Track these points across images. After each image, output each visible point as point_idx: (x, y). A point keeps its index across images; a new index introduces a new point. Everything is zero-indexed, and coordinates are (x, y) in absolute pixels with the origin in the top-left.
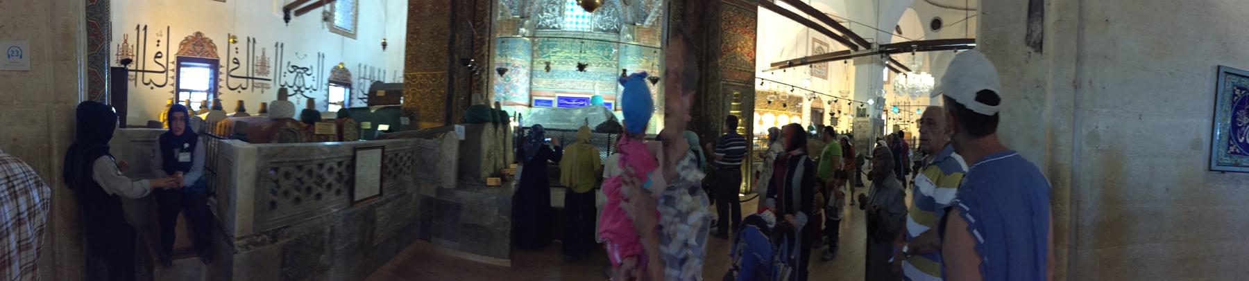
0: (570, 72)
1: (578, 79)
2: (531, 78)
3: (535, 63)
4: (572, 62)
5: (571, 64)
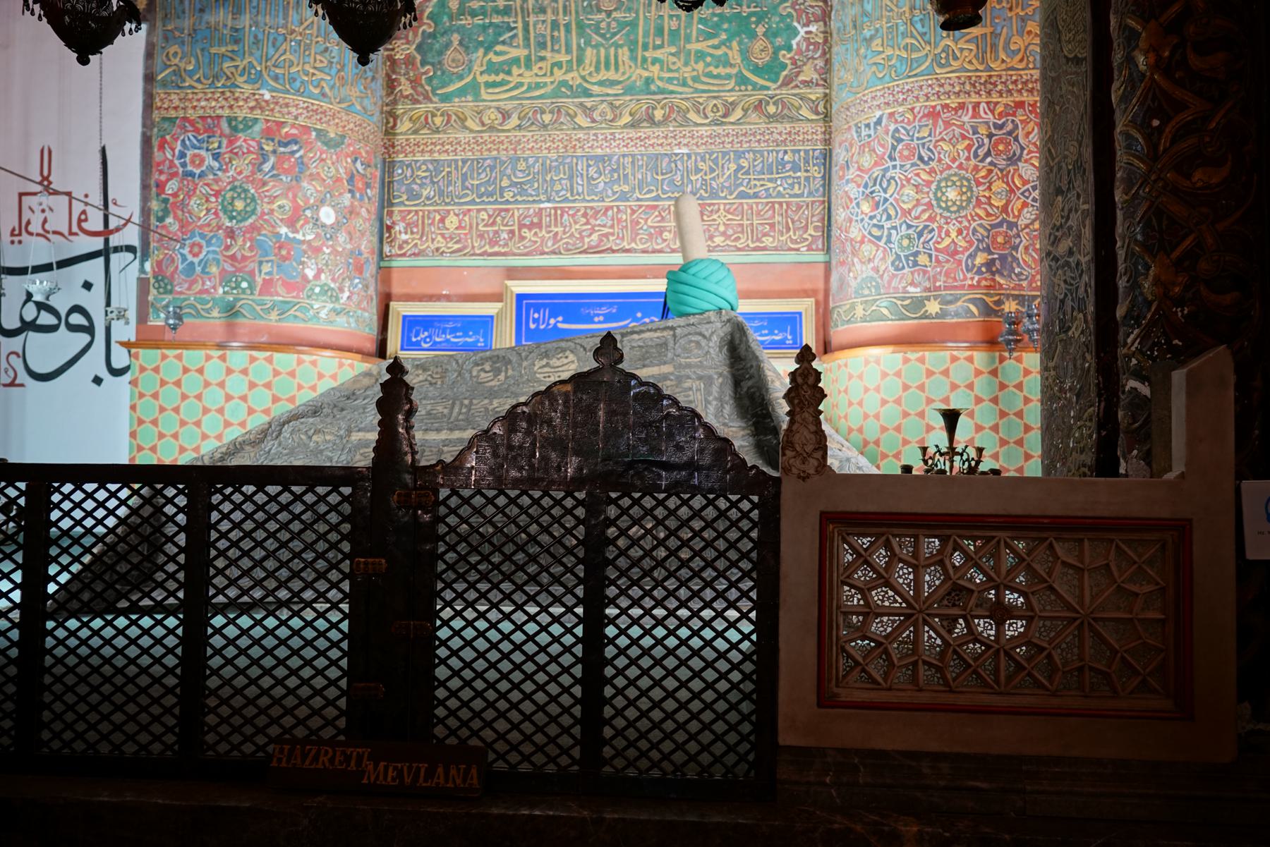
1: (624, 197)
2: (386, 202)
3: (404, 126)
4: (588, 111)
5: (582, 120)
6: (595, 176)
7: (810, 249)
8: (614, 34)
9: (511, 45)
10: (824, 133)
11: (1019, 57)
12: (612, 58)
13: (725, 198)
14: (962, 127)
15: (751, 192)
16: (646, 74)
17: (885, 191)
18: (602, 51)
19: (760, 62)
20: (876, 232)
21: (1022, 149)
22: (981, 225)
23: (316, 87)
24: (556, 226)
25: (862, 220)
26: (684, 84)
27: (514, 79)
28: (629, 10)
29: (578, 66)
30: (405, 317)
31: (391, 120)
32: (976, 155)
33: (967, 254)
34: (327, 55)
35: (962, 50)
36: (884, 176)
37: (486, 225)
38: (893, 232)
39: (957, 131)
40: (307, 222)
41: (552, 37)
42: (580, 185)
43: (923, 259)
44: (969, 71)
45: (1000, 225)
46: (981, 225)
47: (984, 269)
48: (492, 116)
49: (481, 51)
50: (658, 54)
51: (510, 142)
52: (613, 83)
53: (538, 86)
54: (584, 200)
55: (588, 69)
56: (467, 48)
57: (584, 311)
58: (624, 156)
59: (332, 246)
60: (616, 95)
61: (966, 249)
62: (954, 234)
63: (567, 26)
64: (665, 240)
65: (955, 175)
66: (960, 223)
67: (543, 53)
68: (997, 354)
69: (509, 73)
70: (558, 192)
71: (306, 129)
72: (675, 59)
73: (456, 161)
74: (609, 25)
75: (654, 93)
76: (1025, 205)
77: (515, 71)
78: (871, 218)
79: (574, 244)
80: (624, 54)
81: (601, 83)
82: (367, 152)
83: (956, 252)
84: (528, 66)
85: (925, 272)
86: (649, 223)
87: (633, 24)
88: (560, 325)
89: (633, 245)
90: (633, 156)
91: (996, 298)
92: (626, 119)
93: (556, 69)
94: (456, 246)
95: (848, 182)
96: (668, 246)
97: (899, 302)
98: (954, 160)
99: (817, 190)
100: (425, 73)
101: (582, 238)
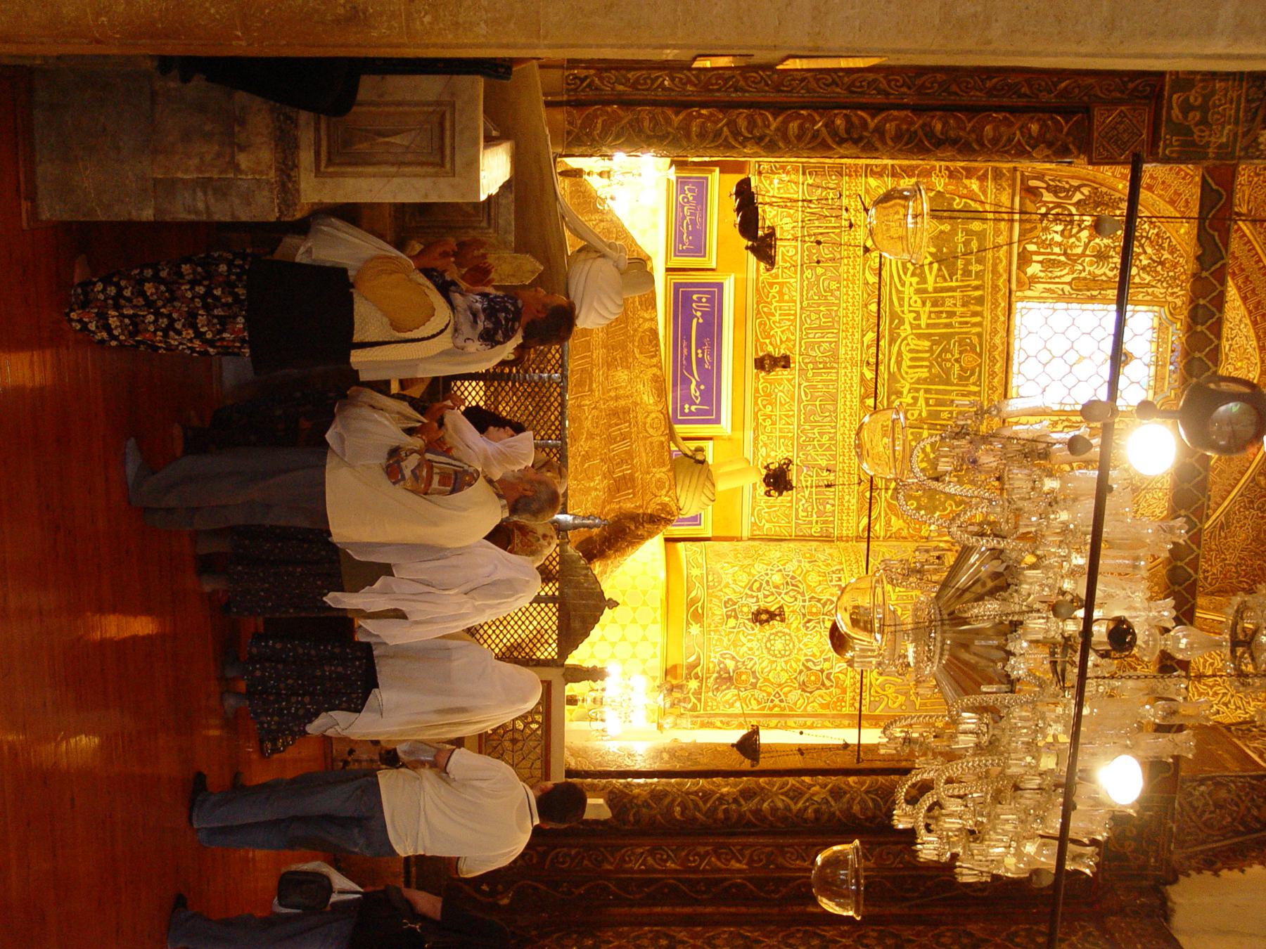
0: (830, 336)
6: (822, 349)
7: (754, 524)
8: (940, 366)
9: (937, 276)
10: (848, 536)
11: (879, 690)
12: (921, 363)
15: (802, 478)
16: (905, 391)
17: (786, 593)
18: (927, 355)
20: (756, 585)
21: (811, 693)
22: (755, 664)
24: (780, 315)
25: (767, 574)
27: (908, 279)
28: (960, 378)
29: (915, 334)
30: (707, 178)
31: (879, 170)
32: (808, 661)
33: (734, 654)
36: (798, 592)
38: (755, 600)
41: (942, 312)
42: (814, 336)
43: (732, 622)
45: (755, 677)
46: (755, 664)
47: (722, 666)
49: (933, 250)
50: (921, 402)
51: (854, 275)
52: (899, 364)
53: (901, 300)
54: (801, 339)
55: (914, 342)
56: (937, 238)
57: (707, 341)
58: (837, 373)
61: (738, 653)
62: (749, 645)
63: (947, 326)
64: (765, 407)
65: (794, 646)
67: (928, 304)
68: (658, 675)
69: (913, 275)
70: (809, 316)
72: (916, 416)
74: (949, 360)
76: (769, 694)
77: (915, 280)
78: (768, 582)
79: (765, 331)
80: (924, 373)
81: (899, 353)
83: (735, 645)
84: (918, 291)
85: (722, 624)
86: (779, 394)
87: (948, 382)
88: (695, 321)
89: (762, 381)
90: (837, 381)
93: (915, 315)
95: (800, 561)
96: (760, 410)
97: (700, 604)
98: (805, 645)
99: (801, 530)
101: (768, 337)
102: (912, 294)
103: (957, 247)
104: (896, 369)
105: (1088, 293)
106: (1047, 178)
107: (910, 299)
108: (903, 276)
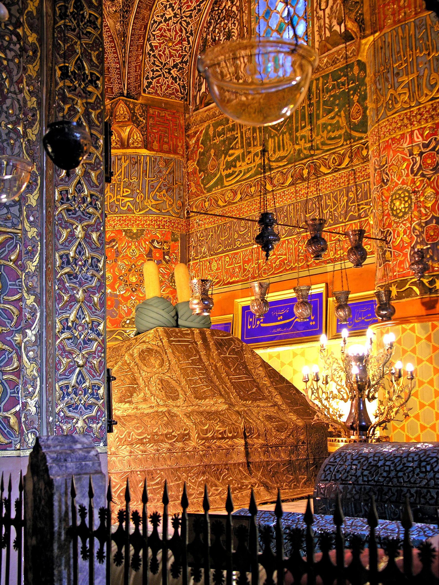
9: (235, 149)
13: (343, 222)
14: (402, 153)
16: (297, 147)
18: (276, 138)
19: (356, 121)
23: (124, 207)
26: (318, 149)
34: (131, 187)
35: (400, 94)
37: (228, 266)
39: (400, 155)
40: (120, 284)
41: (253, 137)
44: (406, 109)
45: (430, 221)
48: (229, 194)
49: (223, 158)
53: (248, 171)
58: (289, 205)
59: (137, 295)
60: (284, 166)
65: (399, 189)
66: (405, 225)
69: (235, 166)
71: (120, 232)
73: (215, 227)
75: (303, 159)
77: (238, 164)
79: (269, 269)
81: (277, 160)
82: (163, 235)
83: (404, 248)
84: (244, 160)
88: (262, 325)
91: (430, 279)
92: (290, 180)
94: (217, 280)
100: (201, 177)
102: (245, 163)
103: (222, 141)
104: (285, 160)
105: (246, 34)
106: (195, 93)
107: (248, 164)
108: (237, 174)
